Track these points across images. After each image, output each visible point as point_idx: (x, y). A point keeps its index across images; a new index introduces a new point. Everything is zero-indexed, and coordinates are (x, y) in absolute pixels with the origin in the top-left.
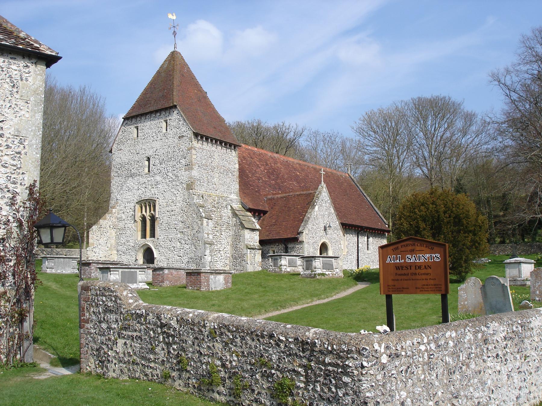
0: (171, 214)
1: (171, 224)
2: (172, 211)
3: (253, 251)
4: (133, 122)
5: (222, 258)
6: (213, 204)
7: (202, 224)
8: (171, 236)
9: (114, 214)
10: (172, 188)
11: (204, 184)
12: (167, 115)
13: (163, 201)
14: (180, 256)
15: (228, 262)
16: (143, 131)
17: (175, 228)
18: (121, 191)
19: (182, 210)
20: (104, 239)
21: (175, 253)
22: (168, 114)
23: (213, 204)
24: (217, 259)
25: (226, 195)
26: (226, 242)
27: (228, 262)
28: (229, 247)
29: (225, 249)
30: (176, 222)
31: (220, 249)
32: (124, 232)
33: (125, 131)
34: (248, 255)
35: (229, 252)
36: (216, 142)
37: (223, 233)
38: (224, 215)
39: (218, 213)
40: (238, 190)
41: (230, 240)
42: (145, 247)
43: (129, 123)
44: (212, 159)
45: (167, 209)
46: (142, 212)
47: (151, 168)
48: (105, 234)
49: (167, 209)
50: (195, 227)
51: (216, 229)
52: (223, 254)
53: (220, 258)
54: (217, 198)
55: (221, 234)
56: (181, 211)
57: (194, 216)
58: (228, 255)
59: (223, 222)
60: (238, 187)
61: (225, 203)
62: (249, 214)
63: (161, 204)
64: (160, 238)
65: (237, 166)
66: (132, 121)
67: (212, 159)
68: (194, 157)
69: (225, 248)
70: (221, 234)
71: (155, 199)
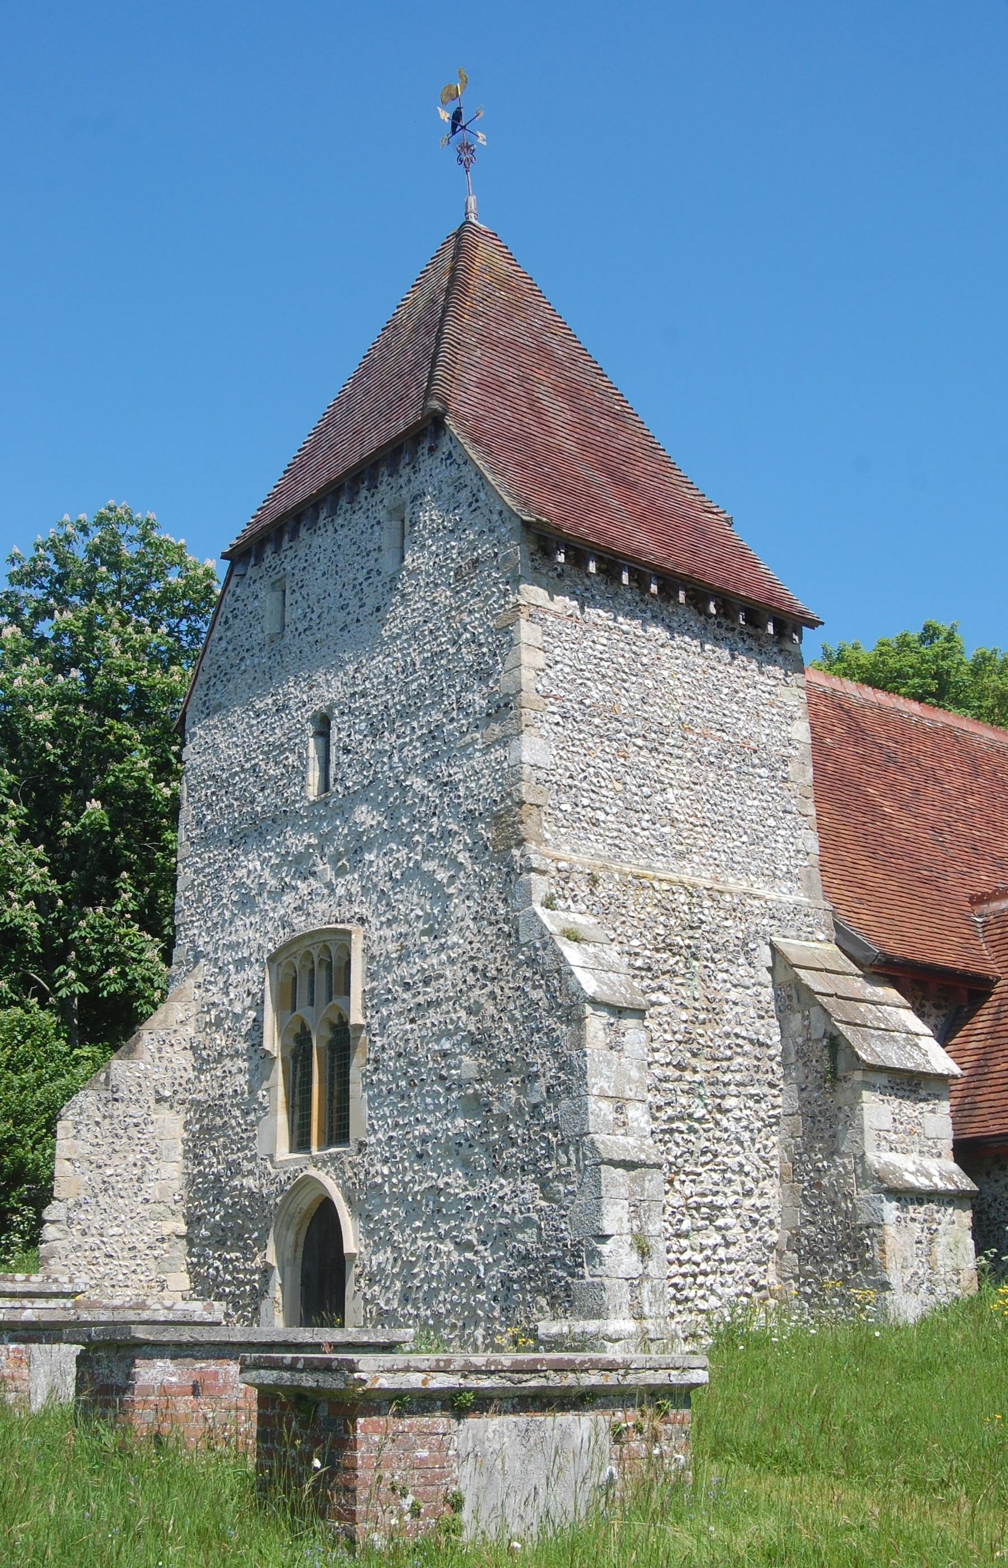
0: (421, 999)
1: (422, 1052)
2: (426, 983)
3: (920, 1212)
4: (266, 564)
5: (733, 1251)
6: (661, 930)
7: (579, 1043)
8: (421, 1129)
9: (181, 1029)
10: (426, 856)
11: (601, 815)
12: (402, 481)
13: (387, 932)
14: (469, 1246)
15: (772, 1279)
16: (304, 592)
17: (442, 1078)
18: (215, 913)
19: (474, 970)
20: (131, 1158)
21: (443, 1227)
22: (406, 472)
23: (661, 930)
24: (698, 1257)
25: (745, 886)
26: (754, 1157)
27: (772, 1279)
28: (772, 1188)
29: (748, 1203)
30: (446, 1045)
31: (719, 1200)
32: (219, 1121)
33: (236, 617)
34: (891, 1230)
35: (773, 1214)
36: (667, 593)
37: (730, 1102)
38: (734, 995)
39: (696, 982)
40: (814, 859)
41: (774, 1142)
42: (306, 1201)
43: (251, 572)
44: (650, 683)
45: (404, 971)
46: (294, 1009)
47: (332, 773)
48: (133, 1132)
49: (404, 971)
50: (541, 1060)
51: (688, 1076)
52: (737, 1230)
53: (722, 1253)
54: (682, 898)
55: (719, 1109)
56: (471, 979)
57: (535, 995)
58: (773, 1236)
59: (727, 1035)
60: (811, 842)
61: (735, 930)
62: (891, 994)
63: (375, 950)
64: (372, 1139)
65: (801, 731)
66: (259, 559)
67: (650, 683)
68: (531, 659)
69: (748, 1194)
70: (719, 1109)
71: (348, 927)
